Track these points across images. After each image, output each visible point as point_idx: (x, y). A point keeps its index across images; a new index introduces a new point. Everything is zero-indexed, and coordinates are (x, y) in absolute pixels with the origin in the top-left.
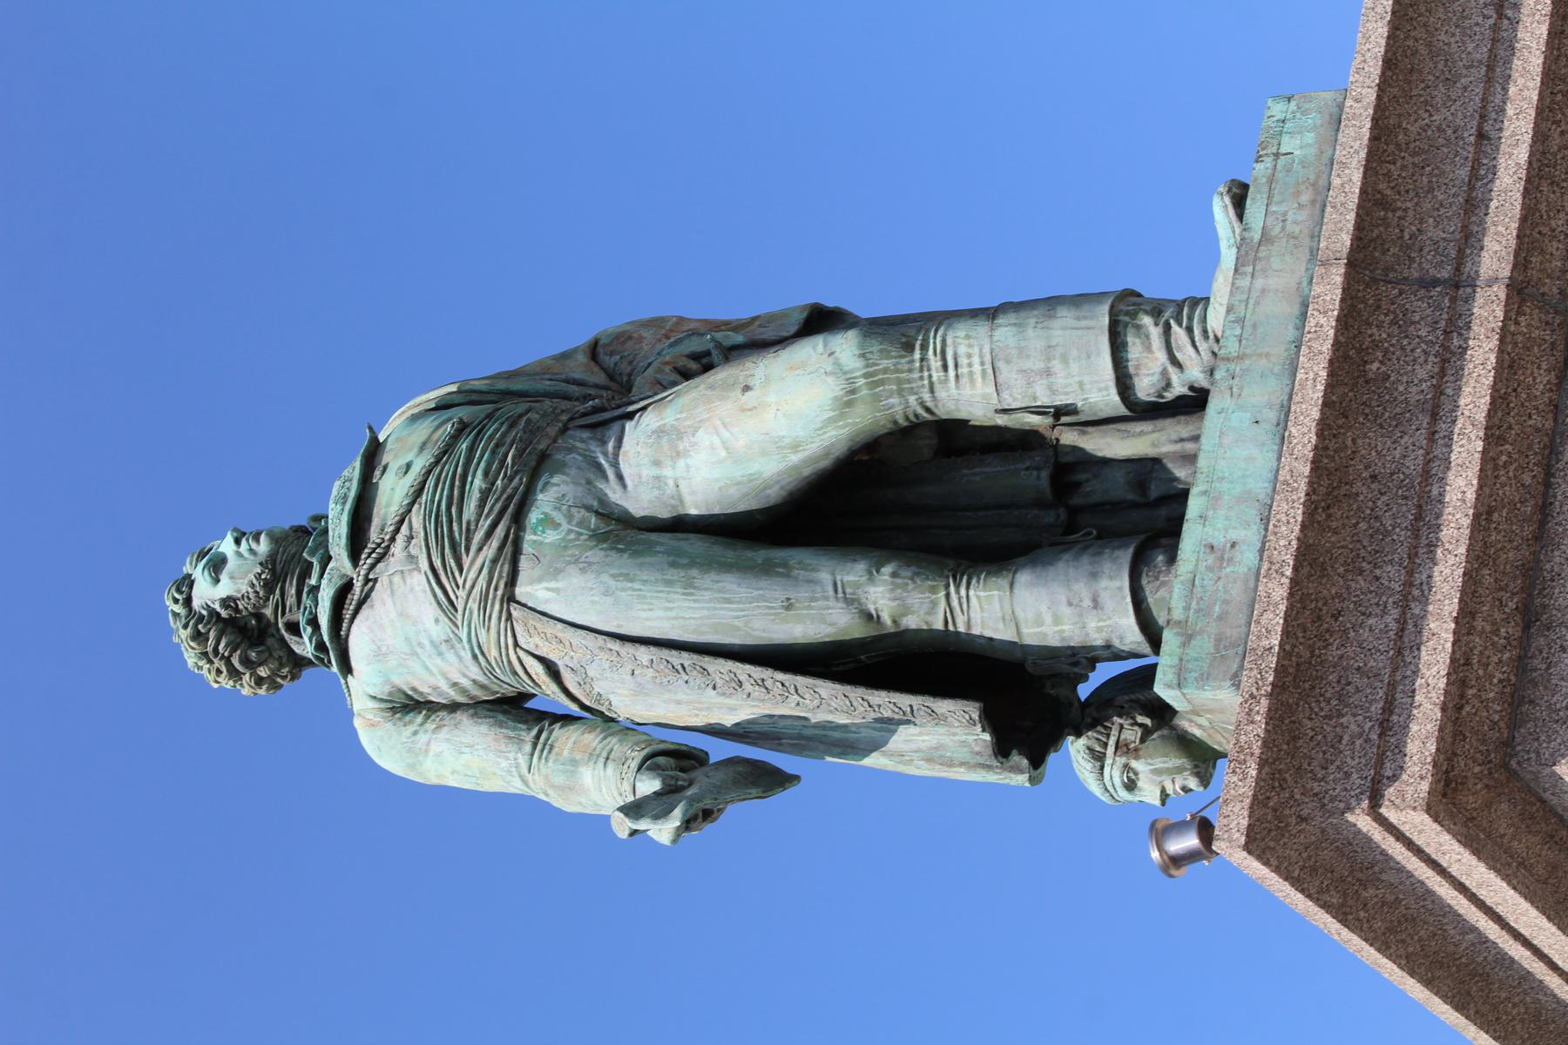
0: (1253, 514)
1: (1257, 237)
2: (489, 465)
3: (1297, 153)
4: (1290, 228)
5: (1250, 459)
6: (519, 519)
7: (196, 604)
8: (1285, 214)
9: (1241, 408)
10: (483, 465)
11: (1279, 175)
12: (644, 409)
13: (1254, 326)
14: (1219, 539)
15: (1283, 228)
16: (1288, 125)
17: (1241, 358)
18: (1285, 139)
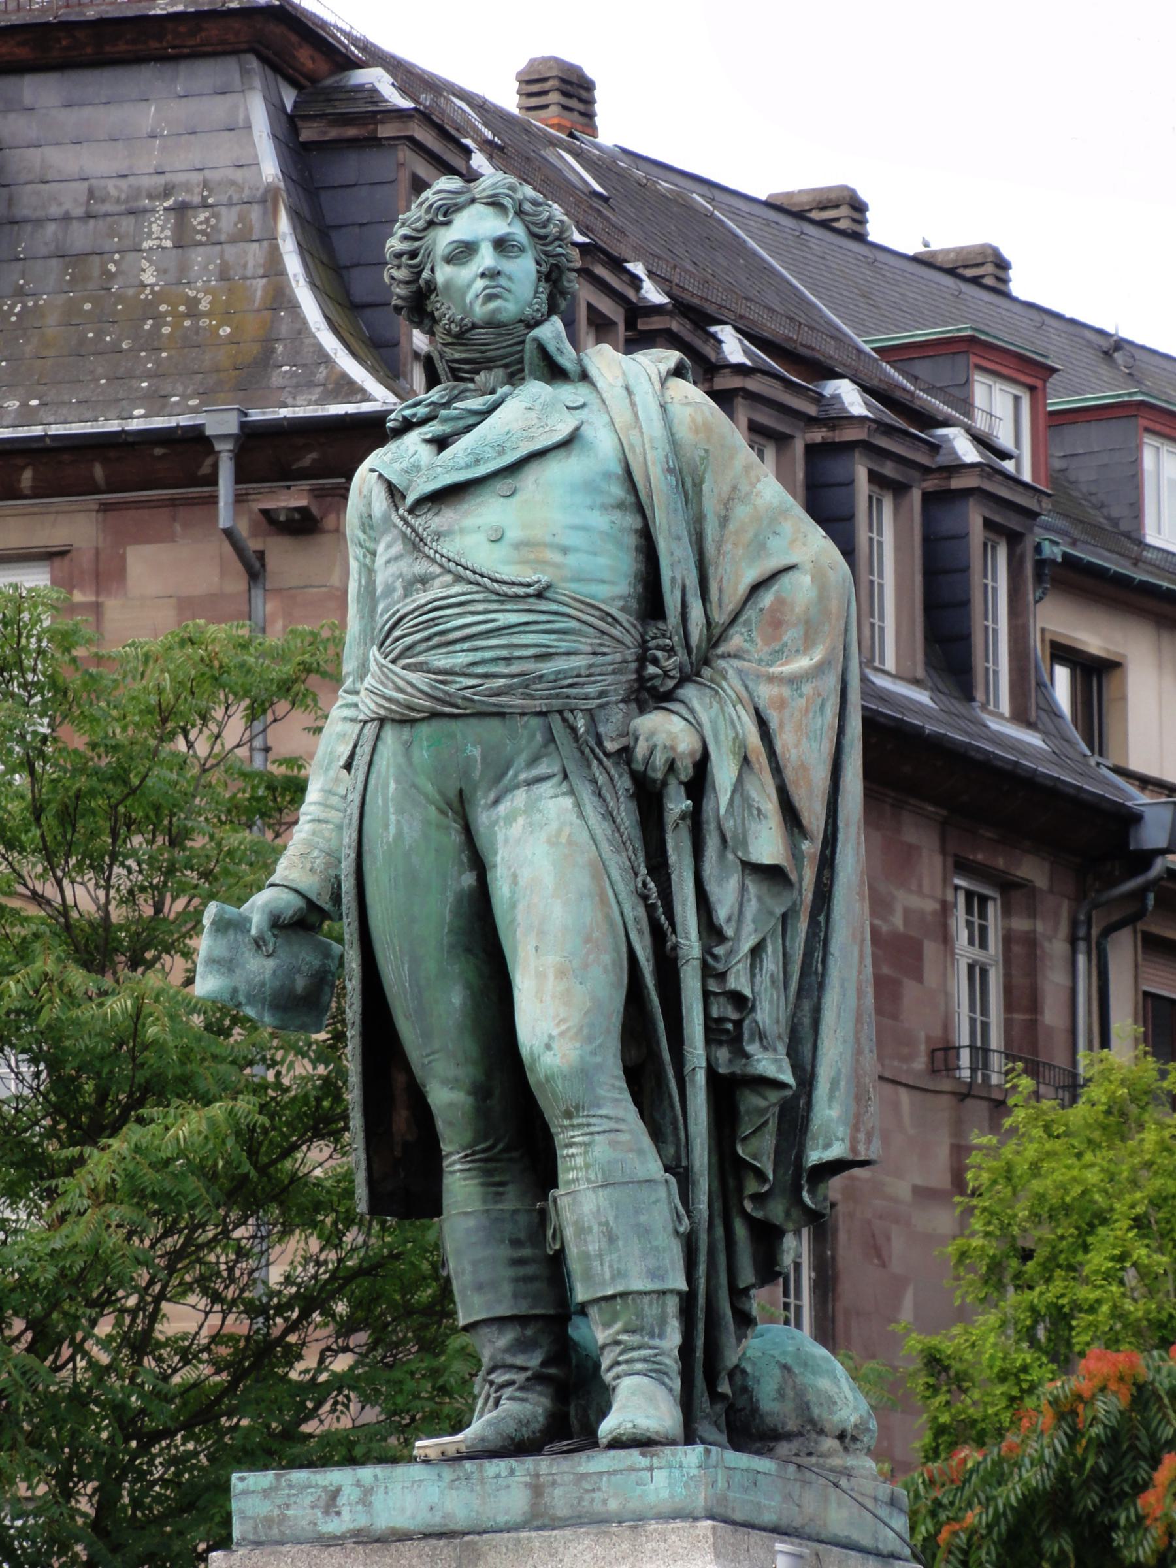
0: (362, 1521)
1: (582, 1469)
2: (483, 662)
3: (652, 1486)
4: (587, 1497)
5: (403, 1510)
6: (434, 715)
7: (431, 234)
8: (599, 1489)
9: (442, 1492)
10: (479, 655)
11: (634, 1476)
12: (572, 792)
13: (508, 1487)
14: (341, 1500)
15: (587, 1491)
16: (677, 1472)
17: (482, 1481)
18: (665, 1472)
